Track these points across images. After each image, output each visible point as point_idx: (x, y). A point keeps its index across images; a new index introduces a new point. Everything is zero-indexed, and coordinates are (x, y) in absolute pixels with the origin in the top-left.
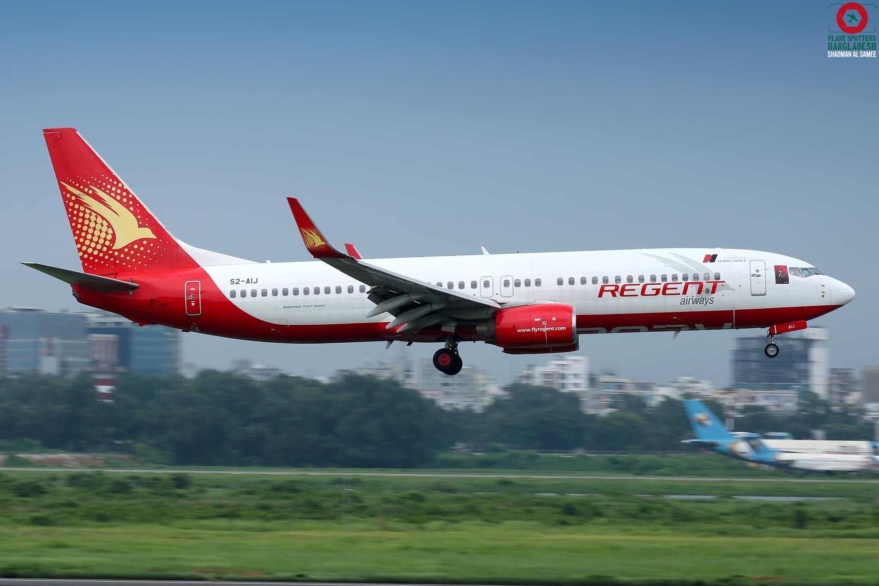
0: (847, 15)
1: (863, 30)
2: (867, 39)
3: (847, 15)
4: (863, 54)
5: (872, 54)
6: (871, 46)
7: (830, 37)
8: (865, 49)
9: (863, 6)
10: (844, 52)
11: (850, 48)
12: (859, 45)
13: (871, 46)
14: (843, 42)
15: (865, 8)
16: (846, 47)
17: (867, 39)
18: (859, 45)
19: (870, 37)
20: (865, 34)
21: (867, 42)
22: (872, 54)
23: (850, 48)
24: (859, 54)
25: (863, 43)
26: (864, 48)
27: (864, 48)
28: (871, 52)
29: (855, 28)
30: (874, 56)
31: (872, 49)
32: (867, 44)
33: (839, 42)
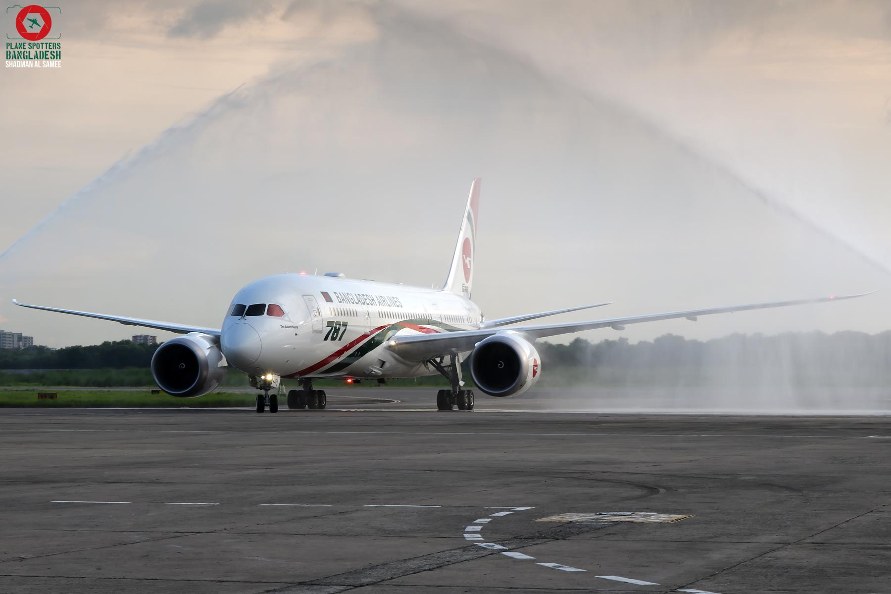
0: (29, 20)
1: (47, 37)
2: (51, 47)
3: (29, 20)
4: (46, 64)
5: (56, 64)
6: (55, 54)
7: (8, 45)
8: (48, 58)
9: (47, 9)
10: (24, 62)
11: (31, 57)
12: (42, 53)
13: (55, 54)
14: (23, 50)
15: (47, 10)
16: (27, 56)
17: (51, 47)
18: (42, 53)
19: (54, 45)
20: (48, 41)
21: (50, 50)
22: (56, 64)
23: (31, 57)
24: (41, 64)
25: (46, 52)
26: (47, 57)
27: (47, 57)
28: (56, 61)
29: (37, 34)
30: (59, 67)
31: (57, 58)
32: (51, 52)
33: (18, 50)
